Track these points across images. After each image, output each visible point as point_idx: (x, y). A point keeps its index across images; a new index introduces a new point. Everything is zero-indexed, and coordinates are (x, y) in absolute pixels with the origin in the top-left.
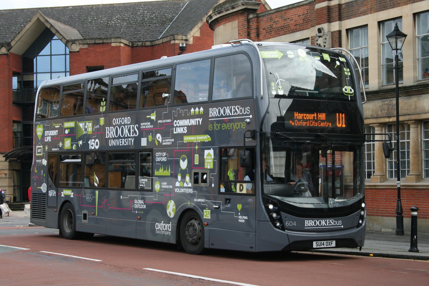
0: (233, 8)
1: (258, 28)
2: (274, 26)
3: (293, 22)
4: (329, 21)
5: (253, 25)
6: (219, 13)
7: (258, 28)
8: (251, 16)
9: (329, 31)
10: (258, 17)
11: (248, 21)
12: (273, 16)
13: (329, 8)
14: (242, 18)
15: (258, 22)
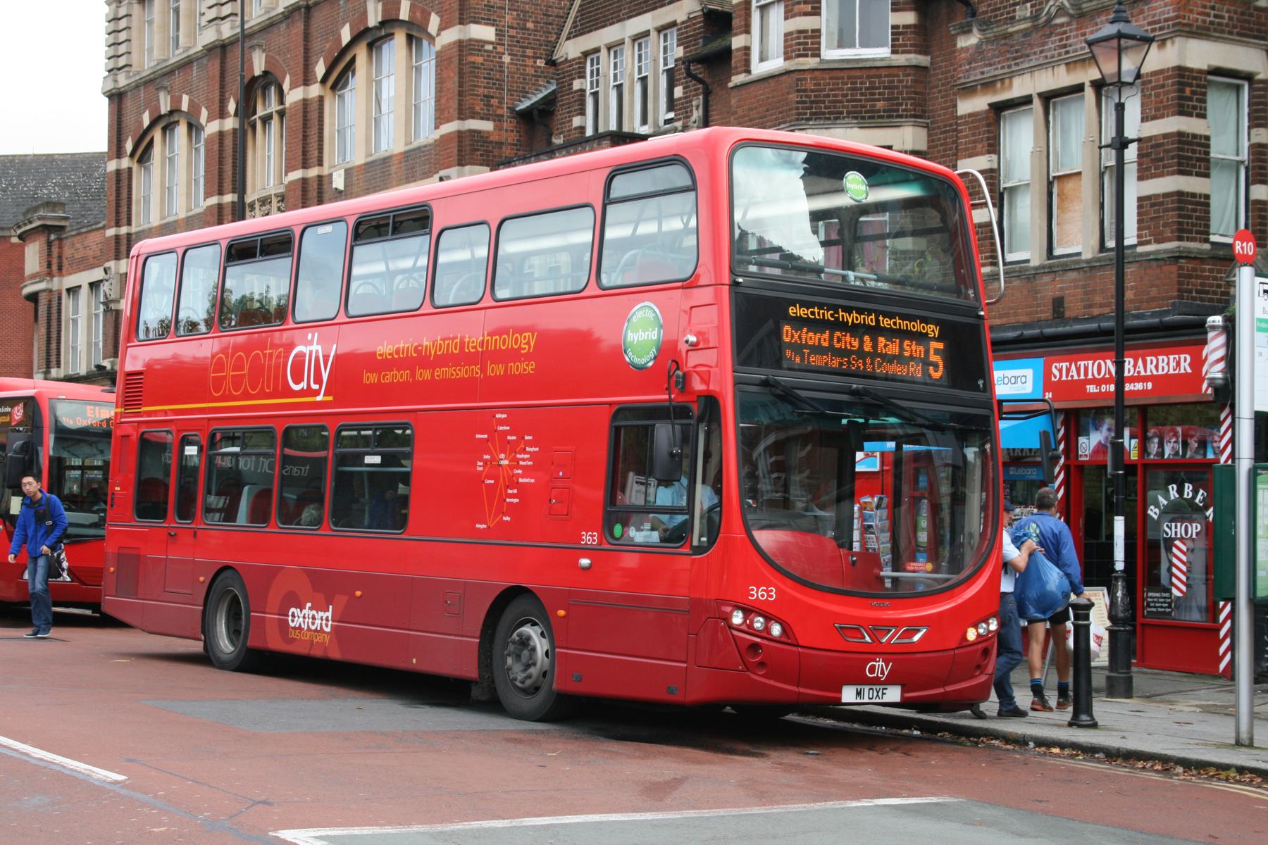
0: (31, 222)
1: (60, 257)
2: (76, 256)
3: (91, 253)
4: (117, 258)
5: (55, 250)
6: (19, 227)
7: (60, 257)
8: (53, 237)
9: (117, 273)
10: (60, 240)
11: (50, 244)
12: (75, 239)
13: (117, 237)
14: (43, 239)
15: (60, 247)
